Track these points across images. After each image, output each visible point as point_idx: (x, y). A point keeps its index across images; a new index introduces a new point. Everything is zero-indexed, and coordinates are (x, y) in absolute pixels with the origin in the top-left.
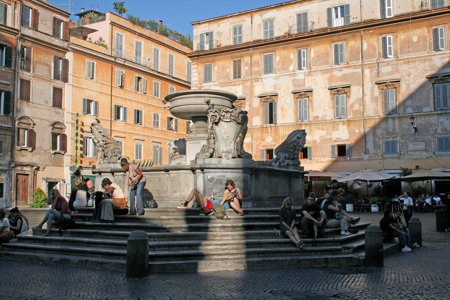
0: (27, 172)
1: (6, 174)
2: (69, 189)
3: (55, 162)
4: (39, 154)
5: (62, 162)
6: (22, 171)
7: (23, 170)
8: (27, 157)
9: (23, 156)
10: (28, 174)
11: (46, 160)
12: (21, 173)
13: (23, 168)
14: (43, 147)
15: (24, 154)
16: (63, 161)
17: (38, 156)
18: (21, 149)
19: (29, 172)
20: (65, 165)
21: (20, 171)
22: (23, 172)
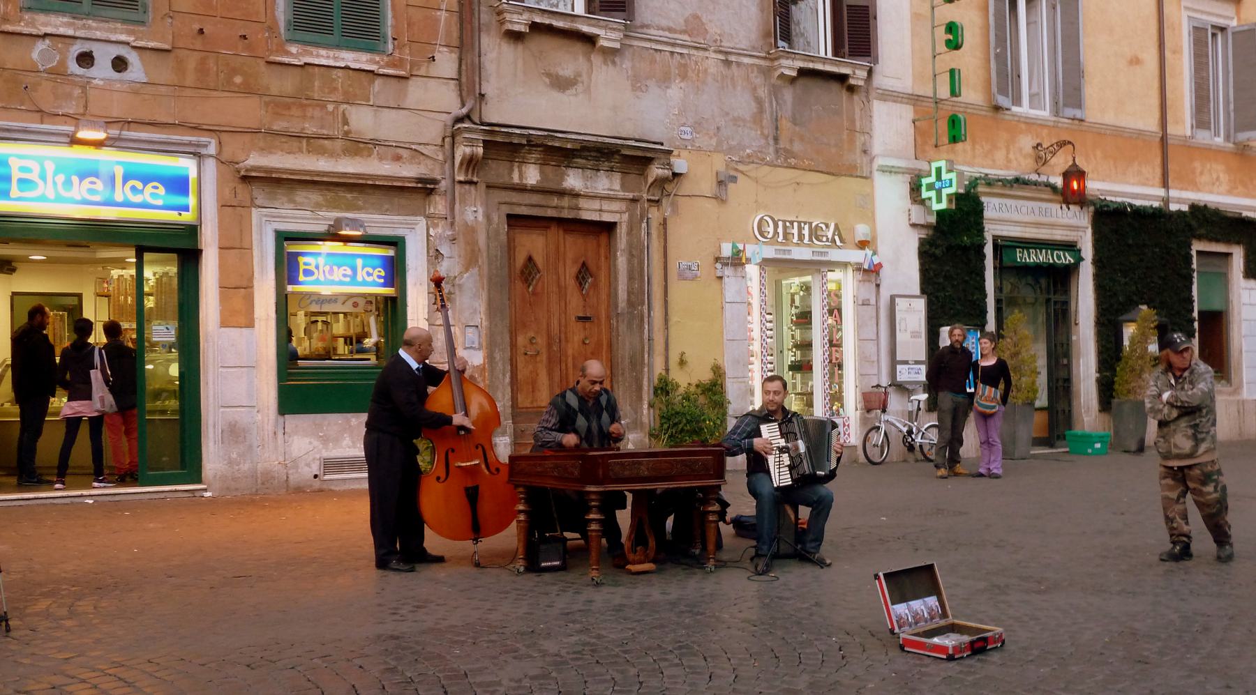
0: (596, 204)
1: (422, 222)
2: (915, 335)
3: (802, 138)
4: (684, 77)
5: (852, 141)
6: (555, 201)
7: (562, 193)
8: (588, 90)
9: (562, 84)
10: (607, 218)
11: (736, 121)
12: (550, 213)
13: (562, 178)
14: (713, 30)
15: (567, 71)
16: (860, 139)
17: (675, 92)
18: (535, 27)
19: (606, 205)
20: (879, 162)
21: (536, 199)
22: (566, 202)
